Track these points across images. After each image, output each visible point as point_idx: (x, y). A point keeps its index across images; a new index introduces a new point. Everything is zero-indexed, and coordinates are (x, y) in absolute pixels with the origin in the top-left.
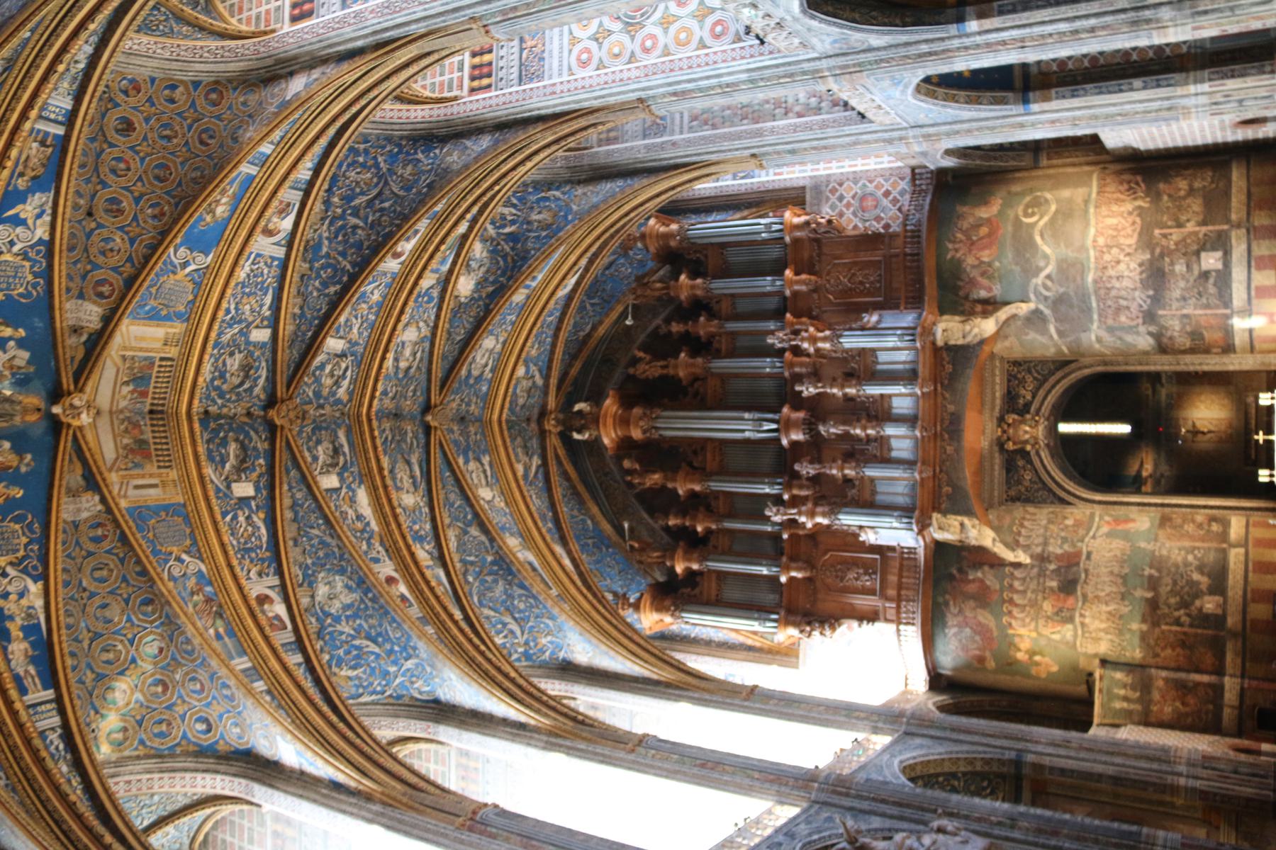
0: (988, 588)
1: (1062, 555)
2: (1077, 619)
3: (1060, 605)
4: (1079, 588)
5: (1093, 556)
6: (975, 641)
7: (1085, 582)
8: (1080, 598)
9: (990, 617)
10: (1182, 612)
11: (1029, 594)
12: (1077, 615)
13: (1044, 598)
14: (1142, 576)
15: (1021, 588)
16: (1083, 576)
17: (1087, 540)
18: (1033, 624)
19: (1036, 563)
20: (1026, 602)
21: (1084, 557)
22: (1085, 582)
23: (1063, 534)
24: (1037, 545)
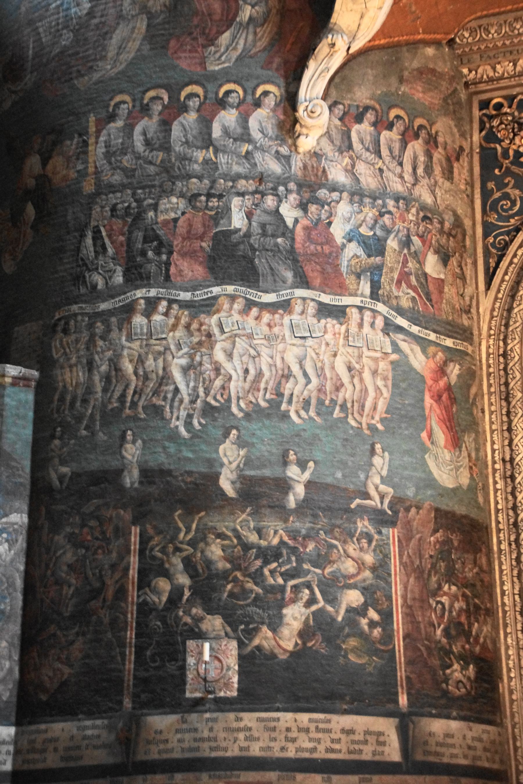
0: (211, 41)
1: (329, 240)
2: (139, 293)
3: (177, 243)
4: (230, 289)
5: (330, 323)
6: (58, 35)
7: (250, 304)
8: (200, 295)
9: (127, 56)
10: (184, 580)
11: (200, 155)
12: (153, 293)
13: (193, 199)
14: (285, 463)
15: (216, 132)
16: (270, 298)
17: (381, 307)
18: (117, 178)
19: (297, 164)
20: (178, 148)
21: (326, 299)
22: (250, 304)
23: (392, 243)
24: (351, 171)
